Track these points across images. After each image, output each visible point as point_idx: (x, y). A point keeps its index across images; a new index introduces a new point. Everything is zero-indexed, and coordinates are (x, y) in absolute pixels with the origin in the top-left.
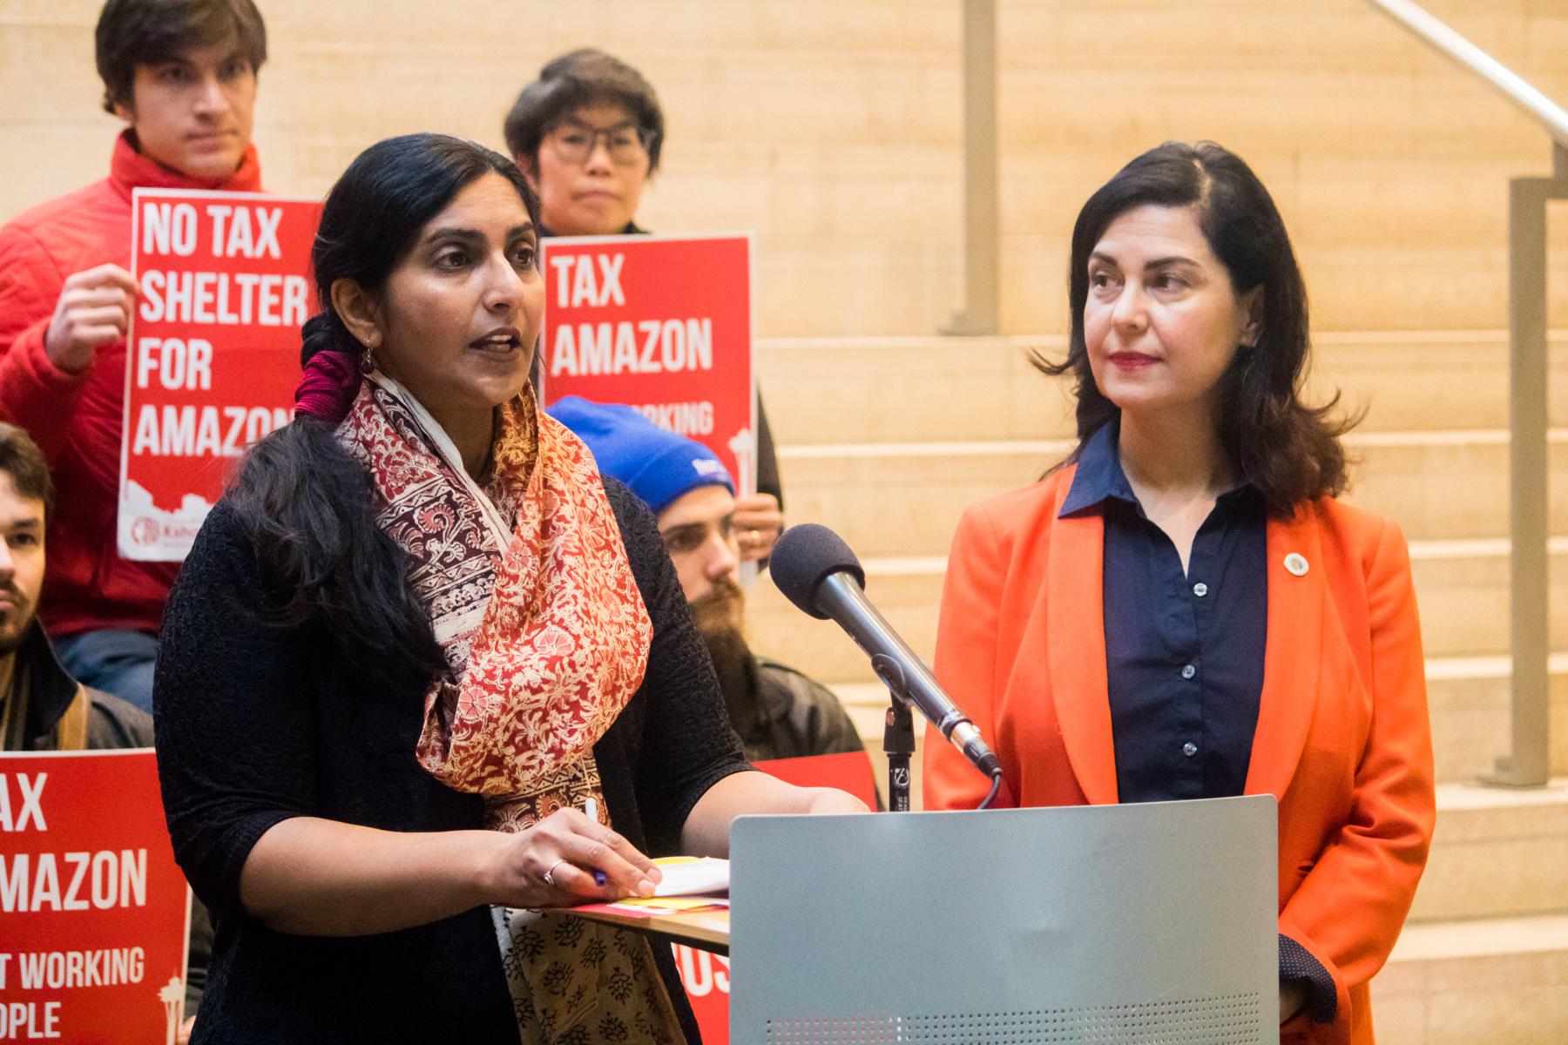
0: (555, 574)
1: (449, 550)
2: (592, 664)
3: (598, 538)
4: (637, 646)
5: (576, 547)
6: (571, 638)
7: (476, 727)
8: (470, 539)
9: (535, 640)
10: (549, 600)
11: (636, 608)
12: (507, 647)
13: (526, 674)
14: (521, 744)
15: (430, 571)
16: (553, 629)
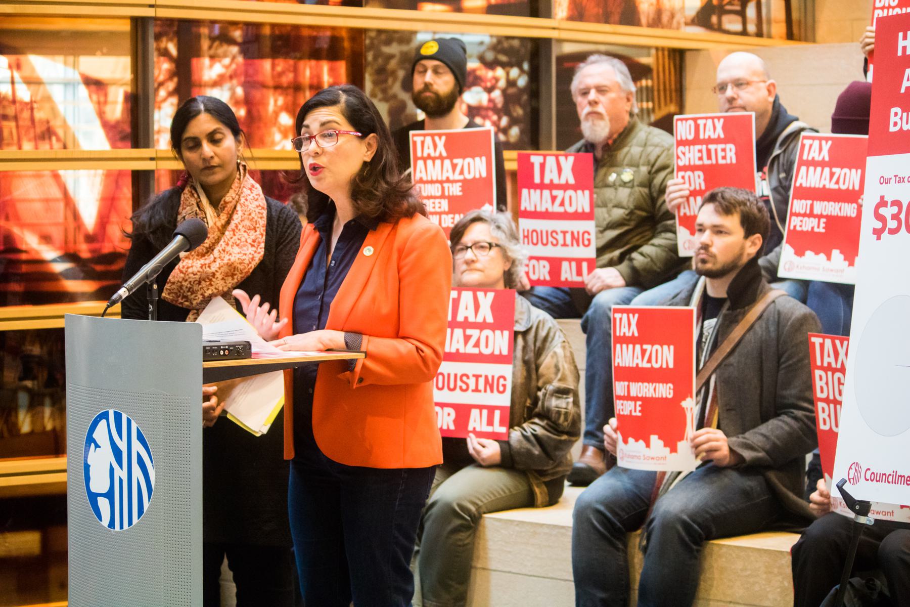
7: (173, 283)
12: (197, 259)
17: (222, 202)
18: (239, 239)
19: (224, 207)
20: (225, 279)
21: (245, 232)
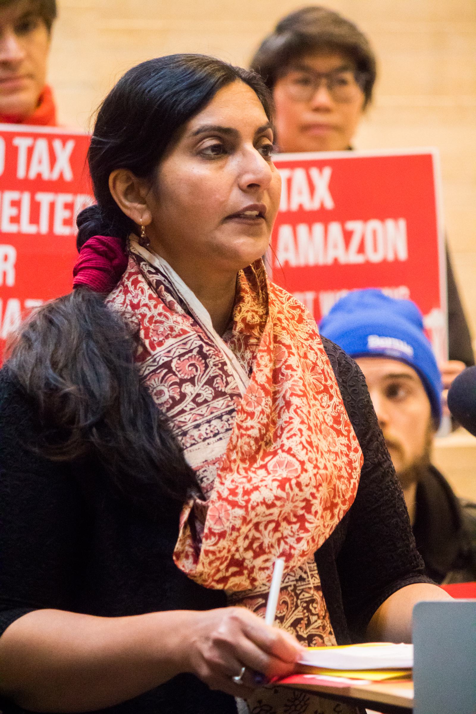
0: (284, 412)
1: (200, 392)
2: (315, 484)
3: (318, 384)
4: (350, 471)
5: (301, 390)
6: (298, 463)
7: (222, 535)
8: (217, 383)
9: (268, 465)
10: (279, 432)
11: (349, 440)
12: (246, 470)
13: (262, 493)
14: (258, 550)
15: (185, 409)
16: (282, 456)
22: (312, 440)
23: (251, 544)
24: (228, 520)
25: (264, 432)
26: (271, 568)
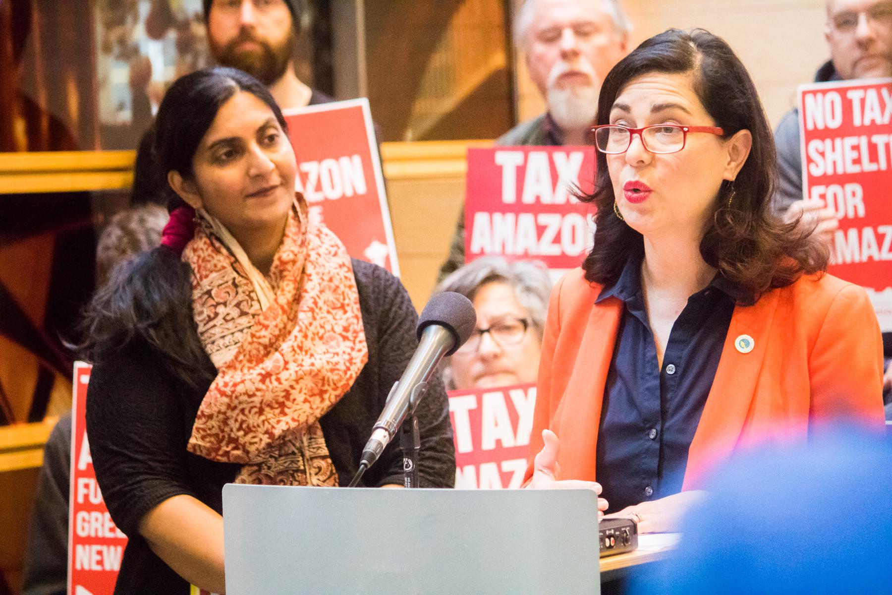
1: (230, 312)
5: (308, 307)
7: (210, 417)
8: (244, 305)
12: (249, 368)
14: (247, 430)
15: (217, 324)
17: (276, 262)
18: (322, 327)
19: (281, 272)
20: (309, 402)
21: (328, 312)
22: (304, 346)
23: (241, 424)
24: (216, 405)
25: (274, 340)
26: (259, 442)
